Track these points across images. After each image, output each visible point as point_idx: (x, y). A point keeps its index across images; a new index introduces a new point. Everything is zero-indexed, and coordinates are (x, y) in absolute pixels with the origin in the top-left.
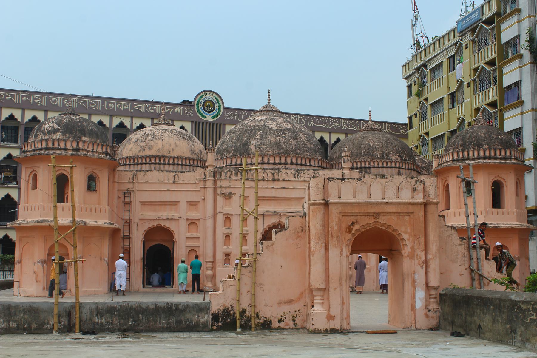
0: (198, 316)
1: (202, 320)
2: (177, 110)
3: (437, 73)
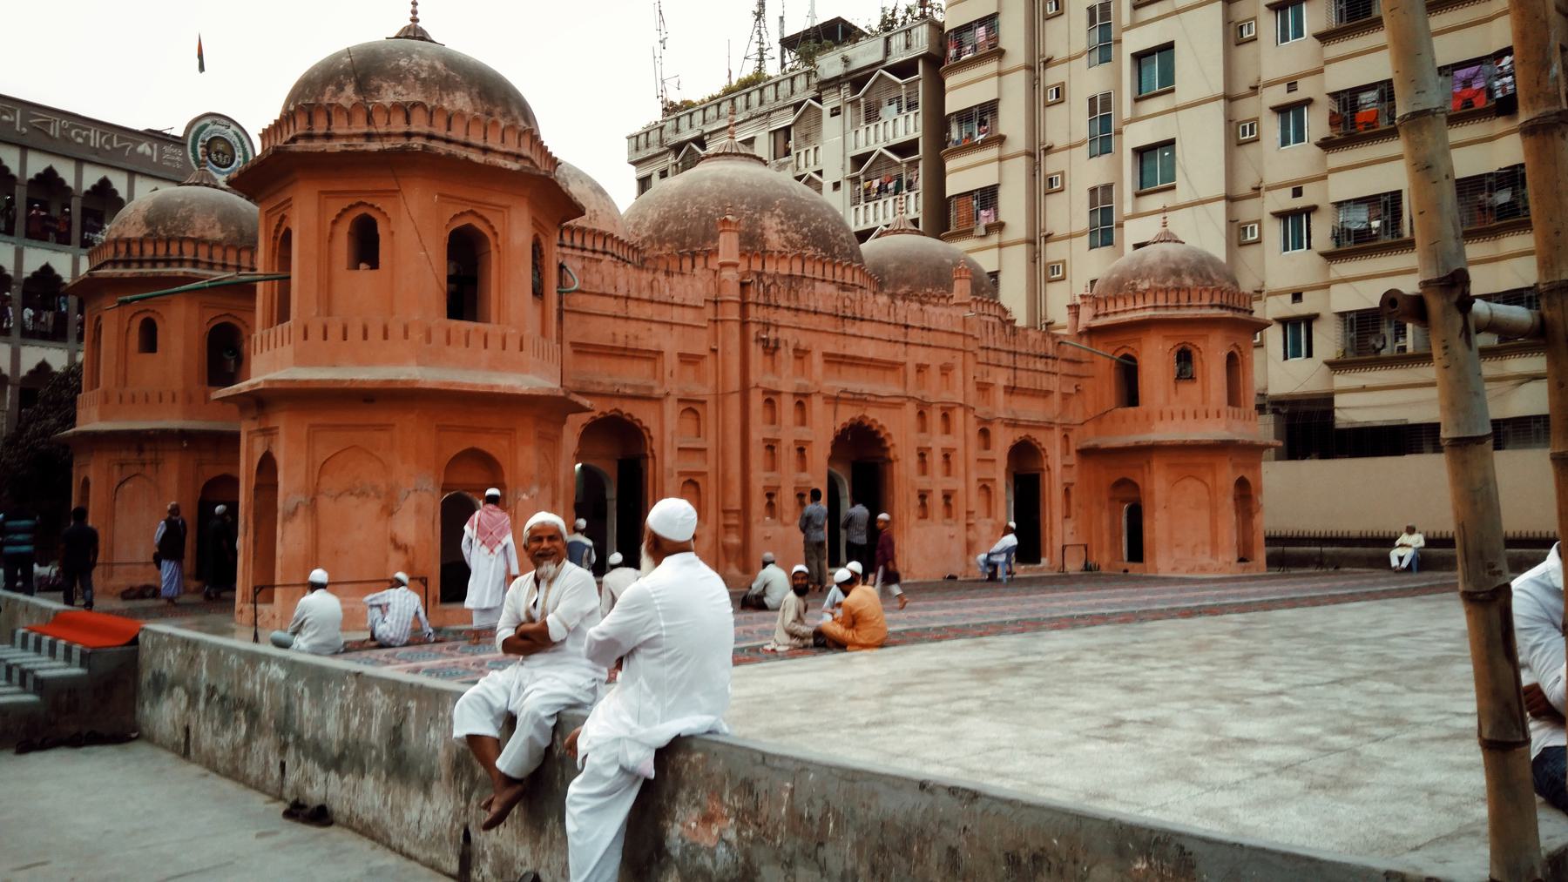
2: (144, 148)
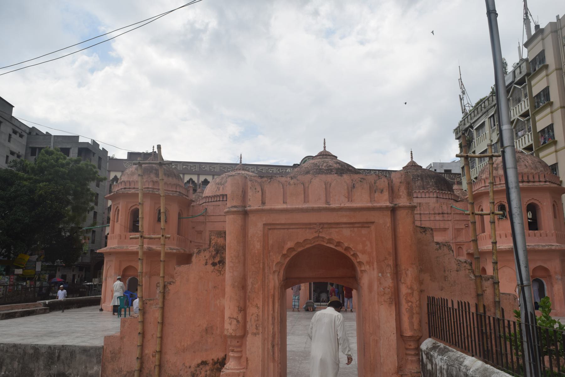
0: (86, 367)
1: (90, 372)
2: (288, 170)
3: (481, 131)
